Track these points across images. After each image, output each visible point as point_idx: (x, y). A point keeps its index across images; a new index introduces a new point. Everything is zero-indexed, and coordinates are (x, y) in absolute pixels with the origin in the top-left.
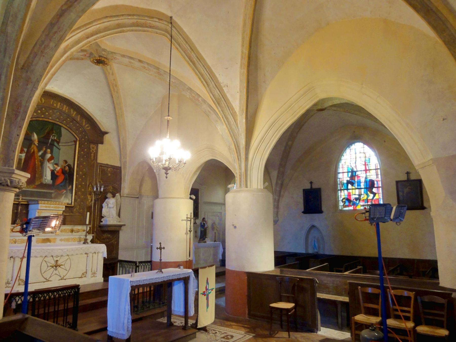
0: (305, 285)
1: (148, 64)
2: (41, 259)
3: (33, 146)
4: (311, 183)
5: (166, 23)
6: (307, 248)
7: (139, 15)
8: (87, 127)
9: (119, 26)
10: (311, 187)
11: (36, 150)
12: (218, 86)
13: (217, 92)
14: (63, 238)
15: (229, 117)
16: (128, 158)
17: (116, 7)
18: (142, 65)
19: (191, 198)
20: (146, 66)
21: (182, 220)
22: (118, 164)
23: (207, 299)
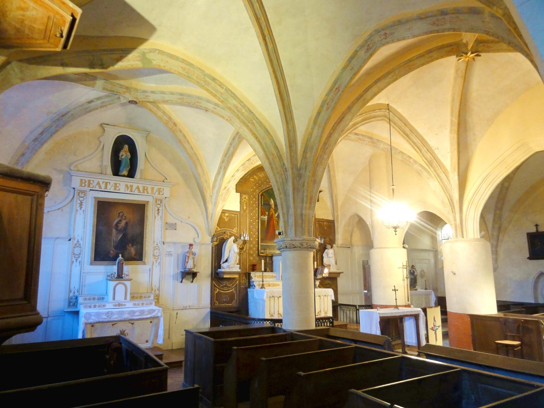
0: (530, 326)
1: (363, 135)
3: (271, 209)
4: (537, 226)
5: (383, 110)
6: (536, 298)
7: (366, 112)
10: (537, 230)
11: (273, 212)
12: (430, 150)
13: (428, 156)
15: (441, 175)
16: (339, 212)
18: (358, 137)
19: (404, 247)
20: (361, 137)
21: (399, 268)
22: (331, 218)
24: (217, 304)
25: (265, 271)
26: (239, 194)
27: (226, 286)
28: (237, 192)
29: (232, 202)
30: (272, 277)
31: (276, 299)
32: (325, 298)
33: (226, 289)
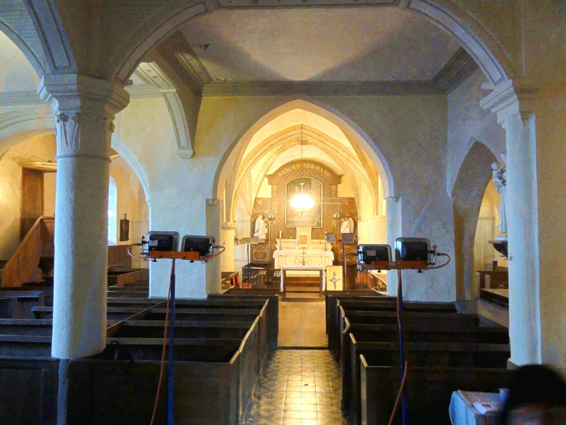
2: (294, 258)
8: (328, 175)
9: (271, 146)
22: (353, 196)
23: (335, 284)
24: (255, 259)
25: (282, 237)
26: (270, 186)
28: (269, 184)
29: (266, 191)
30: (293, 242)
31: (284, 257)
33: (260, 250)
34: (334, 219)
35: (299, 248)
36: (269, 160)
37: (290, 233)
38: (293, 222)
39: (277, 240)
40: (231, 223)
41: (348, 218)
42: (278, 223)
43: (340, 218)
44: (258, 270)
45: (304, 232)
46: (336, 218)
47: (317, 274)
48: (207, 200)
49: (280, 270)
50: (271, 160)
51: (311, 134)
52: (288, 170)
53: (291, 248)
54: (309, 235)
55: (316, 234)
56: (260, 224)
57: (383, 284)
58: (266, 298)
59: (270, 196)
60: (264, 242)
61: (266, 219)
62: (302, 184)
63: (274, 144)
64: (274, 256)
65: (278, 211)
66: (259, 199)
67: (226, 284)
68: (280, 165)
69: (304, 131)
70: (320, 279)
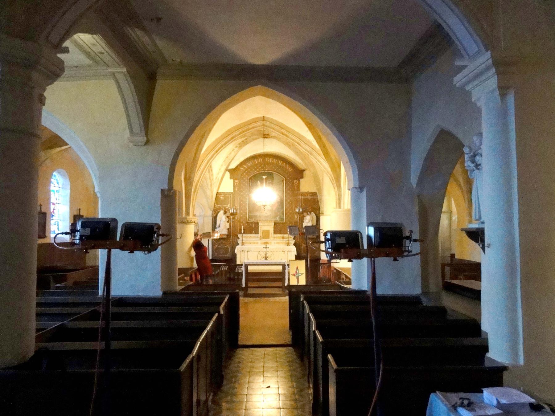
2: (257, 253)
8: (290, 169)
14: (276, 242)
17: (229, 131)
22: (313, 190)
23: (298, 278)
24: (216, 255)
26: (232, 180)
27: (222, 243)
29: (228, 186)
31: (246, 253)
32: (289, 253)
34: (296, 213)
35: (261, 243)
36: (230, 154)
37: (252, 228)
38: (256, 216)
39: (240, 236)
40: (190, 218)
41: (310, 212)
42: (240, 217)
43: (303, 212)
44: (219, 266)
45: (266, 226)
46: (299, 213)
47: (280, 268)
48: (162, 191)
49: (241, 265)
50: (233, 154)
51: (273, 126)
52: (250, 164)
53: (254, 243)
54: (272, 230)
55: (279, 229)
56: (222, 218)
57: (347, 277)
58: (226, 294)
59: (232, 191)
60: (225, 237)
61: (228, 214)
62: (264, 177)
63: (235, 136)
64: (236, 252)
65: (240, 206)
66: (221, 193)
67: (184, 280)
68: (242, 159)
69: (267, 124)
70: (282, 274)
